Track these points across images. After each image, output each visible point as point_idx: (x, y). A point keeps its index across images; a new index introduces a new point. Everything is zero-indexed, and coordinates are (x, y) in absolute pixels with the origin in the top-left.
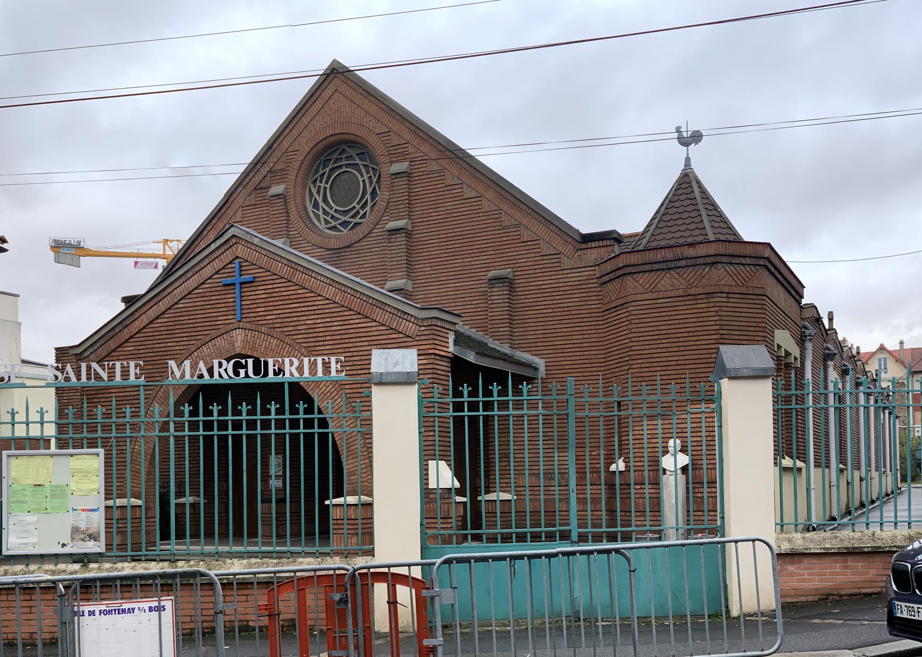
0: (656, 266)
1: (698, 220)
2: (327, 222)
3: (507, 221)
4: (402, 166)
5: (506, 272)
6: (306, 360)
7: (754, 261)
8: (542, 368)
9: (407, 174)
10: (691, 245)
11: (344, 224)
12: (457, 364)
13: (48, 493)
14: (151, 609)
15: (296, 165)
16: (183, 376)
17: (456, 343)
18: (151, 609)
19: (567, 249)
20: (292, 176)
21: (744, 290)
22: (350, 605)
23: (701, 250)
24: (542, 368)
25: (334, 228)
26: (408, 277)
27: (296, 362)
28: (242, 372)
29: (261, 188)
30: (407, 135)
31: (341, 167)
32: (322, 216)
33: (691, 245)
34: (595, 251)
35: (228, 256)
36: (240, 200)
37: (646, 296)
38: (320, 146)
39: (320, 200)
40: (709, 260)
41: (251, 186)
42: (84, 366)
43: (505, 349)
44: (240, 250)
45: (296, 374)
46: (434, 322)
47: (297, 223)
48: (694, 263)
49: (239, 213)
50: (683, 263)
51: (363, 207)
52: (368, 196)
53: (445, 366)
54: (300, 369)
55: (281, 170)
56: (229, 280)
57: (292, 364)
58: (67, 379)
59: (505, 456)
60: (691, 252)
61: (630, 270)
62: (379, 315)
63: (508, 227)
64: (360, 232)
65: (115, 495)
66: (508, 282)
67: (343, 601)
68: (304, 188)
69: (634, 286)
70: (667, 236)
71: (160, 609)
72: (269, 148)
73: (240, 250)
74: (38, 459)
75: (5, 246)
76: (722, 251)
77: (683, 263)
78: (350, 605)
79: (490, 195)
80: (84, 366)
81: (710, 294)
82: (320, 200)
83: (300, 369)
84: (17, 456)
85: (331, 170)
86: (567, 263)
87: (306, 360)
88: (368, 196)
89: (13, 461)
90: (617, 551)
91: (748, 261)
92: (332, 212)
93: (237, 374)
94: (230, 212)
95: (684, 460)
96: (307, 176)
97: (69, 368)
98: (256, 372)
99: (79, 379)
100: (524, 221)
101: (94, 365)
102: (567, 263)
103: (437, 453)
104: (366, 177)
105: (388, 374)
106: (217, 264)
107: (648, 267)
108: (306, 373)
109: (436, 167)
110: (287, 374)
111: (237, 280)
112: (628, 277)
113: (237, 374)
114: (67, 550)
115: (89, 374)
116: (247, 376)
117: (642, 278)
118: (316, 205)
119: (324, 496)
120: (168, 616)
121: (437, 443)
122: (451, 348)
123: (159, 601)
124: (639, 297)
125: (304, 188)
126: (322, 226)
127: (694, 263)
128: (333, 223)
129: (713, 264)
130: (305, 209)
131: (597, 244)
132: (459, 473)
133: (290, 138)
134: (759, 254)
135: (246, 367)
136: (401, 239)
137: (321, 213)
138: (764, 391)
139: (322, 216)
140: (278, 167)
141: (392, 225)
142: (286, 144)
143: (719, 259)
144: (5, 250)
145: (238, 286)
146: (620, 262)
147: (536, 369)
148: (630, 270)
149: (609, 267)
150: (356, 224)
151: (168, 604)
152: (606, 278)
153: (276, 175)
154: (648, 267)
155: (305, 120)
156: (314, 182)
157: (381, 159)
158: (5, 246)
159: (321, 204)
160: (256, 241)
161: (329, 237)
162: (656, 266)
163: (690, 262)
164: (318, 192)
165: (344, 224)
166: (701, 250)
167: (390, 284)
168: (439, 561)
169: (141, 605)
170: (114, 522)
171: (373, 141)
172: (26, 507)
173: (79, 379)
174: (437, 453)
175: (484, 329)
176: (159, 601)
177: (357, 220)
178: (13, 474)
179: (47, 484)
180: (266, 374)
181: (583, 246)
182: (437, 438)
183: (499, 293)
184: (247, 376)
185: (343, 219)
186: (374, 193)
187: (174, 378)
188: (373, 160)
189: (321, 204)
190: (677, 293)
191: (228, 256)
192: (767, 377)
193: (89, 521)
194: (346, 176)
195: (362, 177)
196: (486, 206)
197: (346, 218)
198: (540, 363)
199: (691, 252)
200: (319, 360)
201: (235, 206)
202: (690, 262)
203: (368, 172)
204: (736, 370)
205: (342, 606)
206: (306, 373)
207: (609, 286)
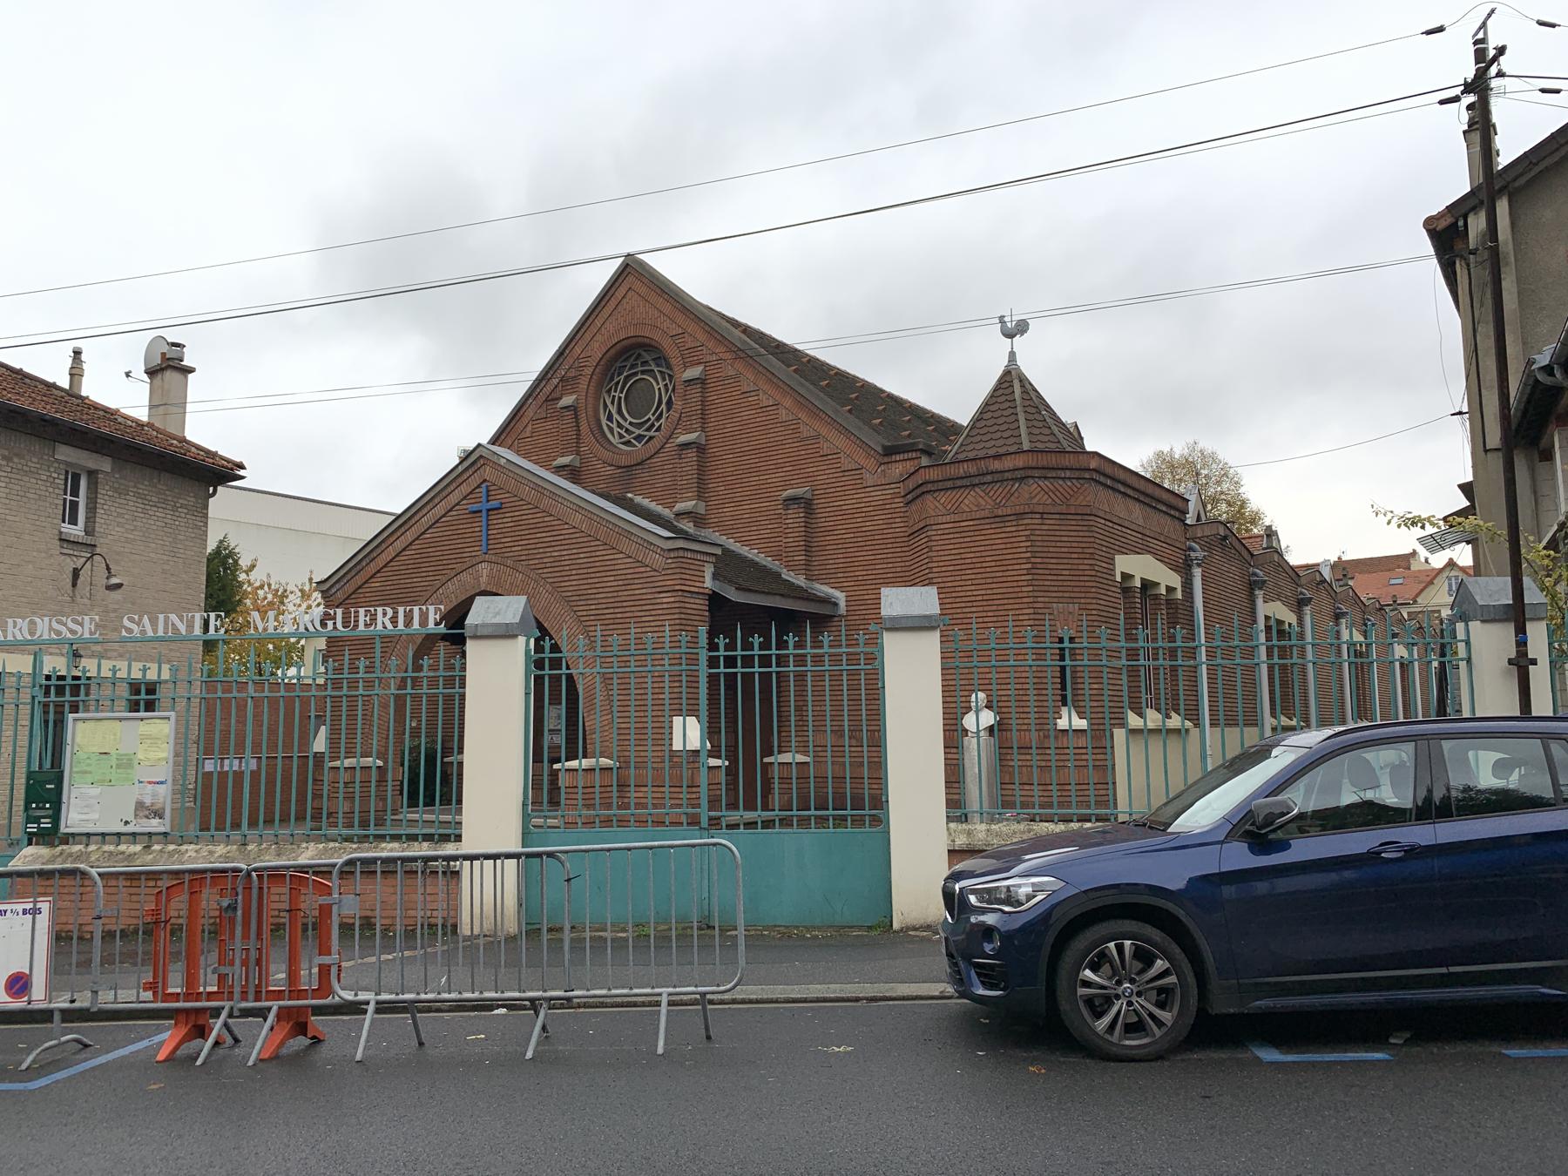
0: (959, 483)
1: (1014, 426)
2: (621, 436)
3: (805, 432)
4: (694, 372)
5: (799, 491)
6: (401, 610)
7: (1077, 474)
8: (842, 604)
9: (701, 381)
10: (997, 457)
11: (639, 438)
12: (715, 600)
14: (25, 912)
15: (588, 371)
16: (265, 629)
17: (715, 576)
18: (25, 912)
19: (870, 463)
21: (1064, 509)
22: (239, 913)
23: (1008, 463)
24: (842, 604)
25: (628, 443)
26: (699, 498)
27: (390, 612)
28: (330, 624)
29: (551, 399)
30: (702, 337)
31: (635, 374)
32: (616, 430)
33: (997, 457)
34: (900, 466)
36: (530, 413)
37: (948, 518)
38: (613, 351)
39: (614, 412)
40: (1018, 474)
41: (542, 397)
42: (161, 617)
43: (800, 581)
44: (487, 472)
45: (390, 626)
46: (681, 553)
47: (587, 437)
48: (1000, 477)
49: (529, 428)
50: (989, 478)
51: (658, 419)
53: (701, 604)
54: (394, 620)
56: (475, 507)
57: (385, 614)
58: (143, 632)
59: (800, 709)
60: (996, 465)
61: (929, 487)
62: (625, 545)
63: (807, 438)
64: (655, 444)
65: (342, 755)
66: (807, 504)
67: (232, 908)
68: (597, 399)
69: (934, 506)
70: (988, 445)
71: (35, 912)
72: (561, 354)
73: (487, 472)
75: (242, 473)
76: (1032, 463)
77: (989, 478)
78: (239, 913)
79: (788, 402)
80: (161, 617)
81: (1020, 515)
82: (614, 412)
83: (394, 620)
84: (84, 720)
85: (627, 378)
86: (870, 479)
87: (401, 610)
89: (80, 725)
90: (550, 855)
91: (1068, 474)
92: (626, 425)
93: (323, 625)
94: (520, 426)
95: (988, 718)
96: (600, 385)
97: (146, 619)
98: (346, 624)
99: (155, 631)
100: (824, 431)
101: (173, 617)
102: (870, 479)
103: (684, 707)
105: (484, 625)
106: (465, 489)
107: (949, 484)
108: (401, 626)
110: (380, 627)
111: (484, 506)
112: (929, 497)
113: (323, 625)
114: (130, 829)
115: (166, 628)
116: (335, 628)
117: (943, 498)
118: (610, 418)
119: (255, 775)
120: (43, 920)
121: (684, 696)
122: (708, 583)
123: (35, 902)
124: (940, 519)
125: (597, 399)
126: (615, 440)
127: (1000, 477)
128: (628, 437)
129: (1023, 478)
130: (599, 421)
131: (901, 457)
132: (711, 731)
133: (582, 344)
134: (1085, 465)
135: (334, 618)
136: (692, 454)
137: (614, 426)
138: (930, 644)
139: (616, 430)
141: (683, 438)
142: (578, 350)
143: (1029, 473)
144: (243, 478)
145: (484, 513)
146: (919, 479)
147: (836, 604)
148: (929, 487)
149: (911, 484)
150: (651, 438)
151: (45, 907)
152: (910, 497)
153: (567, 384)
154: (949, 484)
157: (673, 362)
158: (242, 473)
159: (616, 416)
160: (503, 461)
161: (621, 453)
162: (959, 483)
163: (996, 477)
165: (639, 438)
166: (1008, 463)
167: (680, 507)
168: (340, 861)
169: (14, 907)
170: (341, 785)
171: (666, 344)
172: (89, 778)
173: (155, 631)
174: (684, 707)
175: (777, 557)
176: (35, 902)
177: (652, 433)
178: (78, 740)
179: (113, 752)
180: (356, 626)
181: (886, 460)
182: (684, 690)
183: (795, 516)
184: (335, 628)
185: (638, 432)
186: (669, 403)
187: (256, 628)
188: (669, 367)
189: (616, 416)
190: (983, 514)
192: (933, 628)
193: (154, 795)
194: (642, 384)
195: (658, 386)
196: (784, 415)
197: (640, 432)
198: (840, 597)
199: (996, 465)
200: (416, 609)
201: (525, 420)
202: (996, 477)
204: (893, 619)
205: (230, 914)
206: (401, 626)
207: (914, 507)
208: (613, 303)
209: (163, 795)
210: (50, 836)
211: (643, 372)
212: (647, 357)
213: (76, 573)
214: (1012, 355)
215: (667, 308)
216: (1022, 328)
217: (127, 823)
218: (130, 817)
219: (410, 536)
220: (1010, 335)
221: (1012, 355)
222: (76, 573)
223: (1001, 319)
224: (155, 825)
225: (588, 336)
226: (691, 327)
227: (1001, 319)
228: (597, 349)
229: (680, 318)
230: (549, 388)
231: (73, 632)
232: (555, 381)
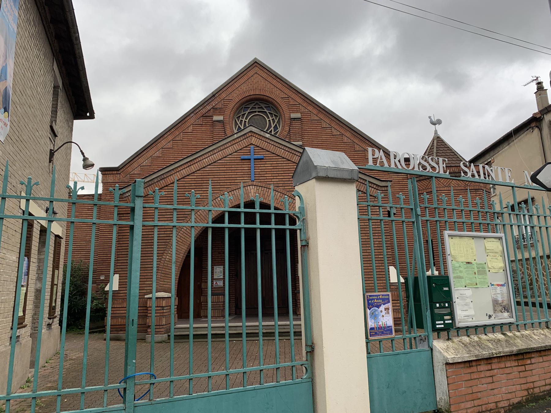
3: (357, 148)
13: (476, 270)
20: (228, 112)
30: (299, 100)
31: (255, 112)
35: (245, 142)
36: (192, 121)
41: (200, 115)
49: (191, 128)
52: (272, 128)
55: (220, 108)
56: (246, 157)
58: (473, 176)
63: (358, 151)
73: (254, 140)
74: (466, 239)
79: (348, 134)
85: (249, 113)
88: (272, 128)
89: (456, 240)
104: (271, 119)
106: (236, 147)
109: (316, 118)
111: (253, 157)
124: (442, 189)
140: (217, 107)
142: (224, 95)
155: (236, 85)
156: (238, 118)
164: (241, 123)
171: (279, 100)
191: (245, 142)
201: (188, 124)
203: (272, 117)
208: (245, 78)
209: (503, 294)
210: (450, 330)
211: (259, 112)
212: (263, 106)
213: (52, 154)
214: (436, 132)
215: (279, 85)
216: (439, 122)
217: (490, 316)
218: (491, 313)
219: (193, 168)
220: (434, 124)
221: (436, 132)
222: (52, 154)
223: (430, 117)
224: (505, 318)
225: (230, 90)
226: (293, 96)
227: (430, 117)
228: (236, 96)
229: (287, 91)
230: (204, 111)
231: (433, 168)
232: (209, 108)
